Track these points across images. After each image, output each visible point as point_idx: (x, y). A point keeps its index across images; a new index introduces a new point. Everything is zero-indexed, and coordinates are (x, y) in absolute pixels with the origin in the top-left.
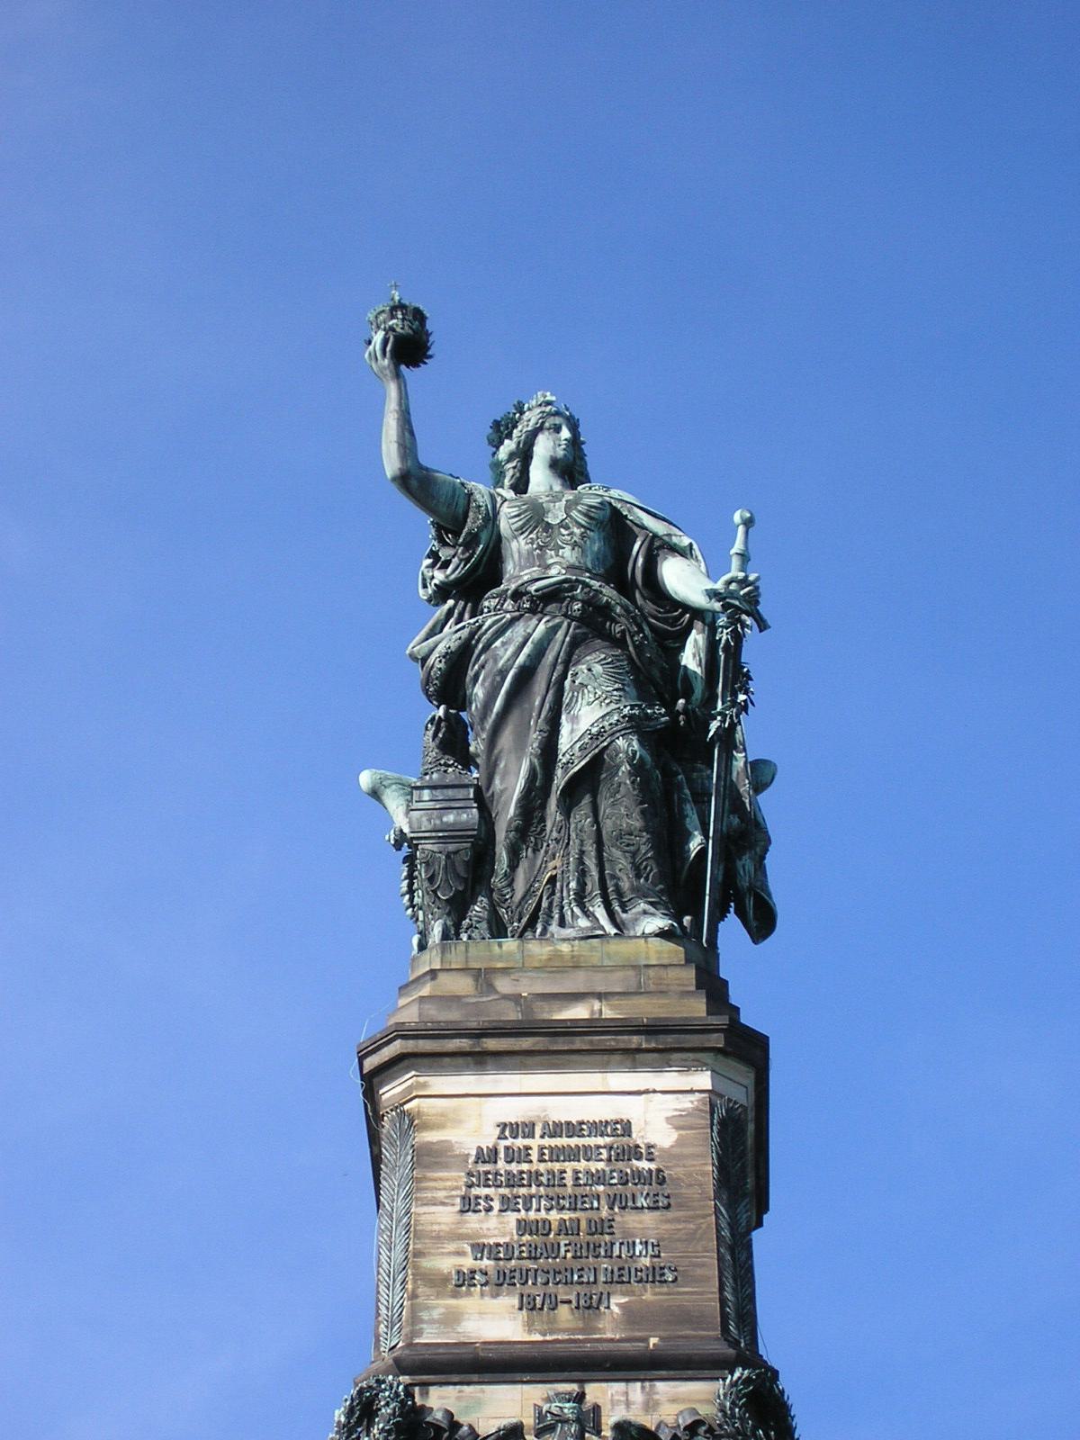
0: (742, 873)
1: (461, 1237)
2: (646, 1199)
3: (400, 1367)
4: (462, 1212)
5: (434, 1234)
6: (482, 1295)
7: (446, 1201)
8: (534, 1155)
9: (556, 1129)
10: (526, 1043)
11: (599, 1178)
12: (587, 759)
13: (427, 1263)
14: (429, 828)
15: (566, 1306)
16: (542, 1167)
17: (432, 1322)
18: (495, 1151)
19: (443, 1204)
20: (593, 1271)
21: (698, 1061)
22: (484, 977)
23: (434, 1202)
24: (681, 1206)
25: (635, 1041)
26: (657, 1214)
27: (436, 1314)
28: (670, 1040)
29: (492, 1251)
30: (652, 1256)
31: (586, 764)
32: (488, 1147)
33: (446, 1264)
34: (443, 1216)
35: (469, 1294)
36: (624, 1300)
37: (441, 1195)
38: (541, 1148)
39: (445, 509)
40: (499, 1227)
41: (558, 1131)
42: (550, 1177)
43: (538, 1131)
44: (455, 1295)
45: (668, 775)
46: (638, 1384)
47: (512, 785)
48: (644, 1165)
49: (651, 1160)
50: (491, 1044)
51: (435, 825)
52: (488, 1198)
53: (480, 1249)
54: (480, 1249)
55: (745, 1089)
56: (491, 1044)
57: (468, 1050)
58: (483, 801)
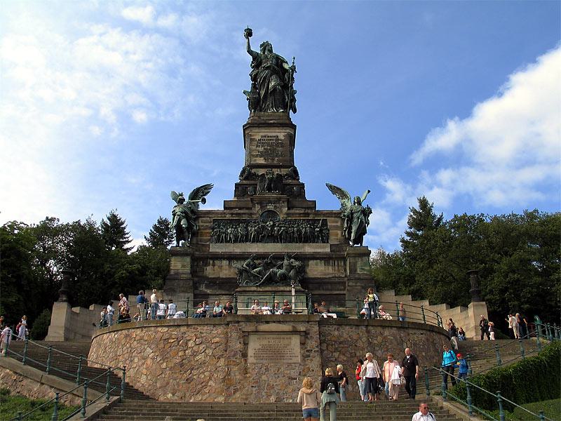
3: (248, 166)
22: (259, 117)
29: (261, 152)
34: (254, 147)
40: (261, 149)
45: (284, 93)
47: (263, 93)
58: (259, 94)
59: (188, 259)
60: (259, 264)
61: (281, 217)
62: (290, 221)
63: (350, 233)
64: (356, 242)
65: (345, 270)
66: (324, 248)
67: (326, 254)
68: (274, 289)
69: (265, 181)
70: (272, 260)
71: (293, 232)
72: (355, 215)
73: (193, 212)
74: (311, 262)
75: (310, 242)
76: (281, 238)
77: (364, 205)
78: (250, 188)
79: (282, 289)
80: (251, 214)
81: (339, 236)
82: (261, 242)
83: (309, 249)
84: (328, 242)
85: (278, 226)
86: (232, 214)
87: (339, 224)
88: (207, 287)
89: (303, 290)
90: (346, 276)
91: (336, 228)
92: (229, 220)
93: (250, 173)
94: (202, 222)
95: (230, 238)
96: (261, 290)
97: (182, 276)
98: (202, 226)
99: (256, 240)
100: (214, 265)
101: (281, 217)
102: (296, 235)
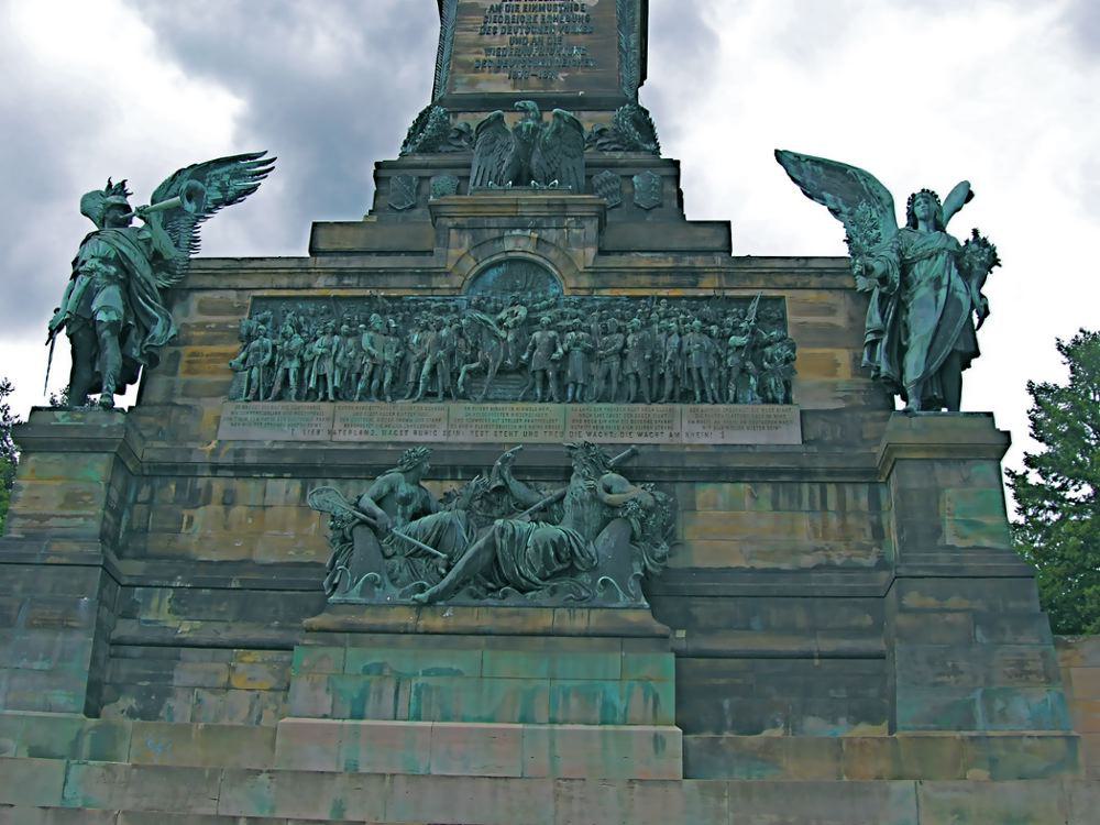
1: (480, 46)
4: (481, 34)
6: (490, 72)
8: (521, 9)
11: (555, 19)
13: (461, 57)
15: (534, 78)
16: (525, 14)
17: (462, 84)
26: (586, 36)
27: (465, 80)
33: (471, 58)
35: (483, 71)
36: (566, 75)
38: (525, 6)
40: (499, 41)
44: (475, 72)
48: (579, 13)
49: (583, 11)
52: (495, 28)
53: (488, 51)
54: (488, 51)
59: (97, 469)
60: (448, 497)
61: (567, 286)
62: (609, 305)
63: (898, 352)
64: (929, 404)
65: (878, 533)
66: (772, 424)
67: (783, 451)
68: (505, 623)
69: (506, 147)
70: (502, 480)
71: (622, 355)
72: (919, 271)
73: (157, 260)
74: (705, 492)
75: (704, 400)
76: (560, 375)
77: (959, 228)
78: (444, 181)
79: (546, 620)
80: (427, 274)
81: (844, 373)
82: (464, 397)
83: (692, 429)
84: (787, 400)
85: (549, 327)
86: (340, 274)
87: (840, 320)
88: (180, 606)
89: (659, 628)
90: (882, 564)
91: (829, 336)
92: (326, 298)
93: (443, 128)
94: (202, 310)
95: (322, 379)
96: (437, 623)
97: (55, 547)
98: (201, 326)
99: (442, 387)
100: (229, 501)
101: (567, 286)
102: (634, 365)
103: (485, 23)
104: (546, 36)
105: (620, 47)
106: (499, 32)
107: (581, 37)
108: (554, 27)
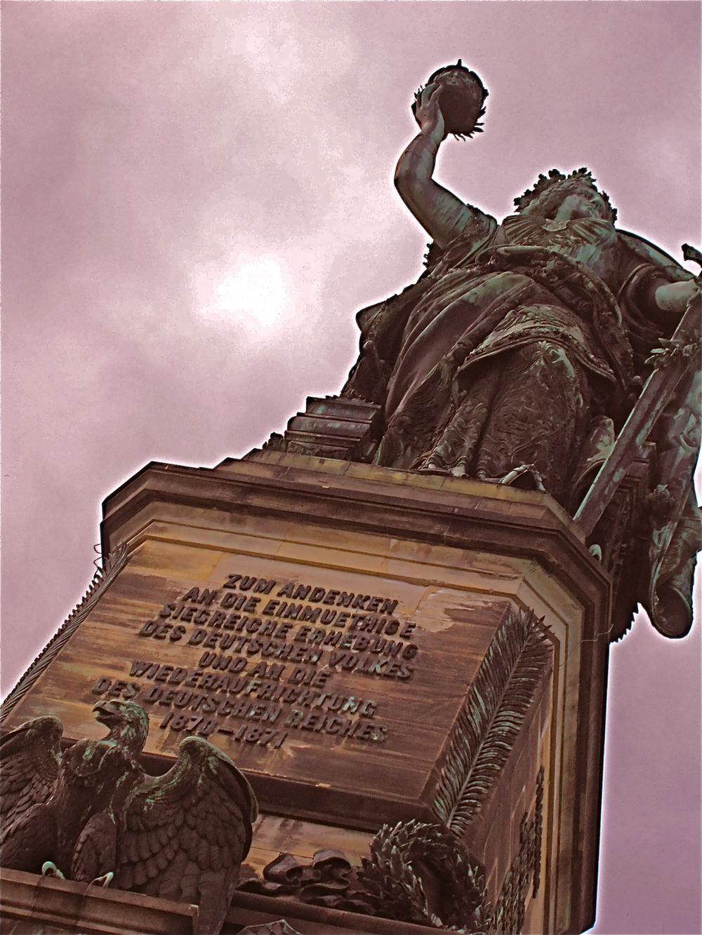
0: (656, 541)
2: (381, 666)
4: (142, 635)
5: (95, 646)
7: (127, 623)
9: (302, 593)
10: (299, 508)
11: (331, 640)
12: (498, 351)
14: (309, 429)
15: (224, 738)
18: (215, 595)
19: (123, 624)
20: (277, 713)
21: (509, 566)
23: (113, 622)
24: (423, 682)
25: (436, 529)
26: (391, 683)
28: (479, 535)
30: (363, 716)
31: (496, 355)
32: (207, 591)
37: (125, 617)
39: (444, 222)
40: (182, 656)
41: (303, 593)
42: (270, 626)
43: (277, 590)
46: (279, 821)
50: (256, 501)
51: (316, 427)
55: (565, 627)
56: (256, 501)
57: (228, 501)
103: (163, 616)
104: (291, 667)
105: (464, 722)
106: (186, 638)
107: (376, 684)
108: (321, 654)
